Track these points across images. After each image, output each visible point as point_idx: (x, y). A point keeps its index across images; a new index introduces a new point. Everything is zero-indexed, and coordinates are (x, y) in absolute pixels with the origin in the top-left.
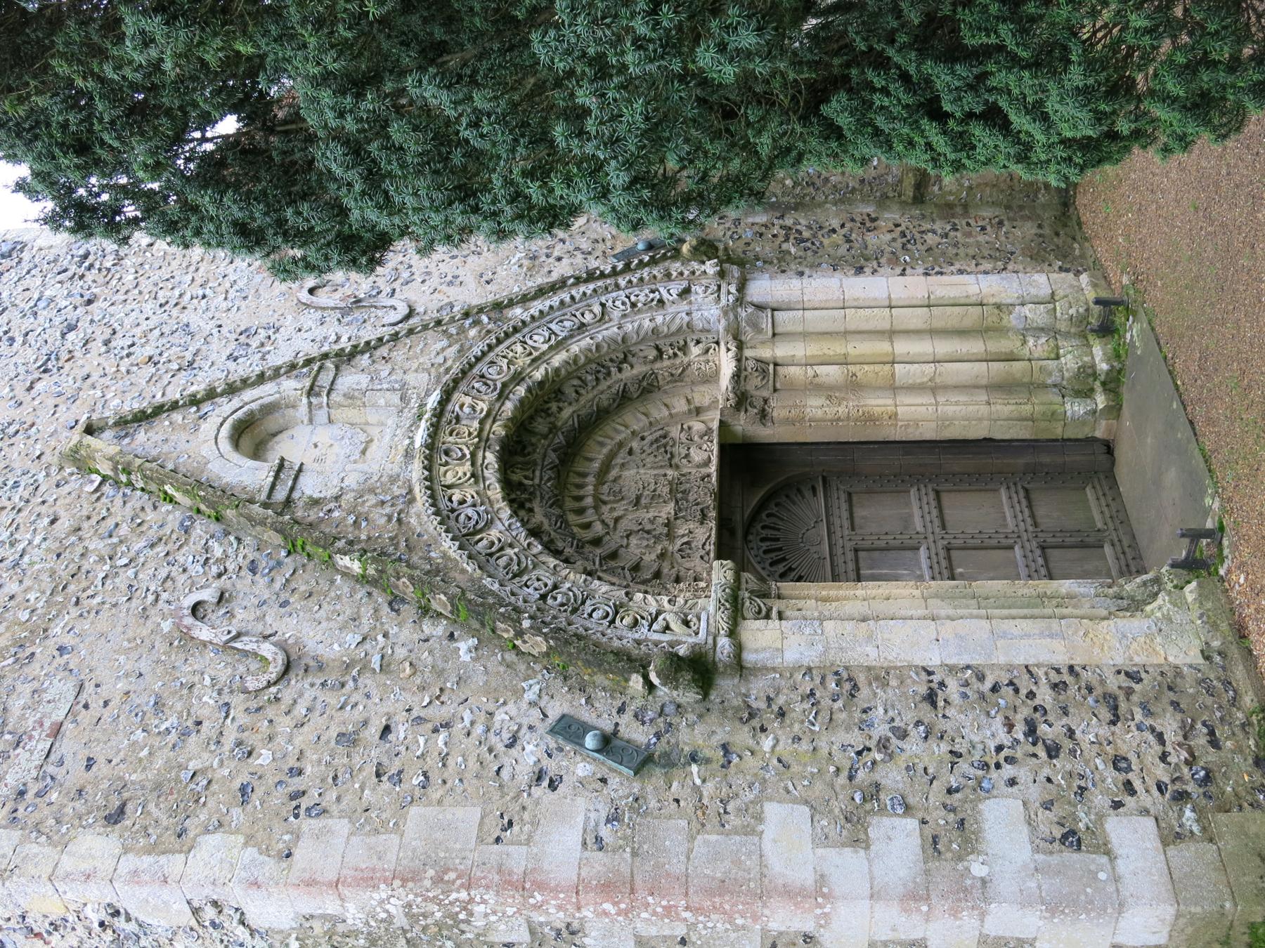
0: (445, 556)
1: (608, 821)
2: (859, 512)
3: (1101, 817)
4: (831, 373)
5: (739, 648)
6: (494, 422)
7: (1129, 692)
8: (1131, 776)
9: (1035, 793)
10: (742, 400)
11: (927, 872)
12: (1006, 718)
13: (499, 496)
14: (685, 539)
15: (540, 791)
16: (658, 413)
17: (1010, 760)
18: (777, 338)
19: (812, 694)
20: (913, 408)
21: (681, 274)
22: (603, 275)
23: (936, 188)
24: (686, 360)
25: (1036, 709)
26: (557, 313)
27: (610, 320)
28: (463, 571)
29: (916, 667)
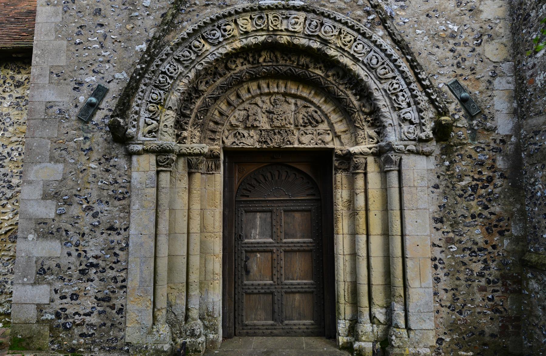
0: (183, 28)
1: (60, 110)
2: (297, 215)
3: (49, 284)
4: (360, 201)
5: (138, 153)
6: (288, 36)
7: (113, 307)
8: (69, 299)
9: (65, 261)
10: (348, 157)
11: (30, 219)
12: (100, 257)
13: (235, 47)
14: (246, 135)
15: (73, 85)
16: (334, 117)
17: (79, 255)
18: (383, 174)
19: (117, 183)
20: (341, 243)
21: (423, 118)
22: (416, 74)
23: (529, 275)
24: (365, 128)
25: (104, 269)
26: (383, 55)
27: (381, 83)
28: (173, 37)
29: (129, 224)
